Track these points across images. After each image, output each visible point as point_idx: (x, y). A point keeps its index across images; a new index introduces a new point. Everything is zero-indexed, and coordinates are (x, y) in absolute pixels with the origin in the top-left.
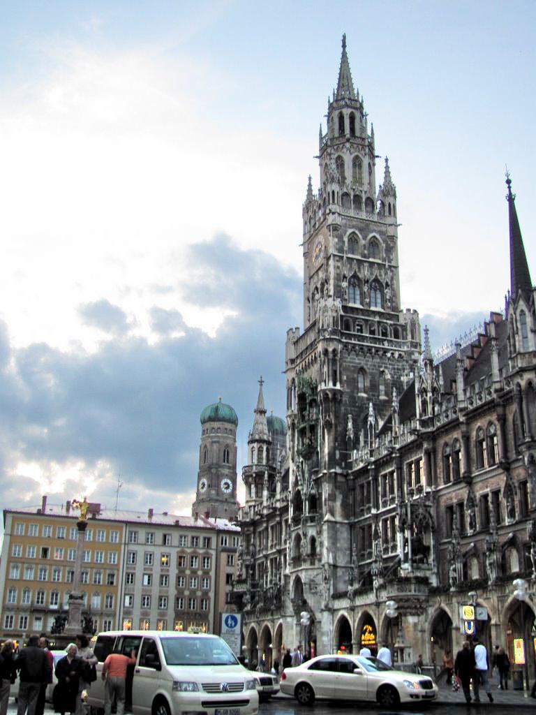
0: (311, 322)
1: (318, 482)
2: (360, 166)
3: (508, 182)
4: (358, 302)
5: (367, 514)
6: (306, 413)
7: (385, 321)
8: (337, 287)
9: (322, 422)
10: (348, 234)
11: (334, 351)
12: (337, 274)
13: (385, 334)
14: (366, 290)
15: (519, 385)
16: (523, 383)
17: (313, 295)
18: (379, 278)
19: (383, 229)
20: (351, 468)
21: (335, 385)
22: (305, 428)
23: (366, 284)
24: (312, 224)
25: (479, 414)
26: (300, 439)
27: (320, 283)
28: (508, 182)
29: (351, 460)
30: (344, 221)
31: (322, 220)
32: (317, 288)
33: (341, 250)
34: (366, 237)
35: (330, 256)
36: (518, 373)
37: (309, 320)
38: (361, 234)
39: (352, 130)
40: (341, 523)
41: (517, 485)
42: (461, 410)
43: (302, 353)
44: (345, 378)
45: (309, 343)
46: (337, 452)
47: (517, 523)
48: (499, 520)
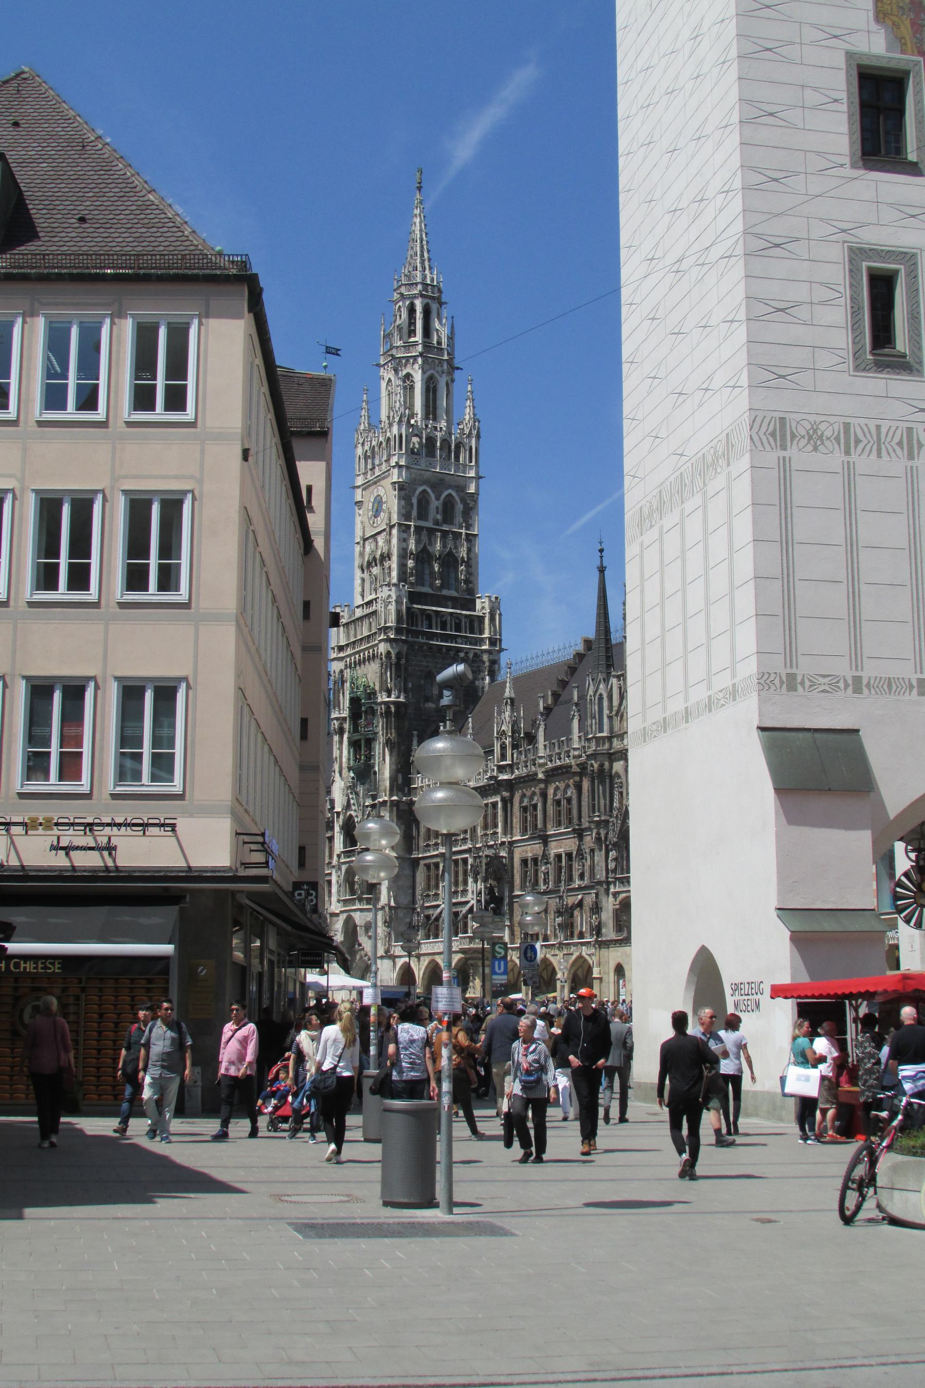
2: (435, 390)
3: (601, 551)
4: (427, 583)
6: (362, 721)
7: (459, 611)
8: (402, 566)
9: (381, 739)
10: (417, 492)
13: (458, 629)
15: (592, 765)
16: (596, 766)
17: (368, 562)
22: (360, 740)
24: (369, 466)
25: (558, 775)
26: (352, 750)
27: (379, 553)
28: (601, 551)
30: (413, 476)
31: (384, 467)
32: (375, 559)
33: (407, 516)
34: (440, 495)
36: (592, 755)
37: (363, 596)
38: (433, 492)
39: (427, 331)
41: (588, 850)
42: (541, 765)
43: (354, 642)
44: (410, 685)
45: (366, 633)
46: (400, 776)
47: (586, 888)
48: (570, 879)
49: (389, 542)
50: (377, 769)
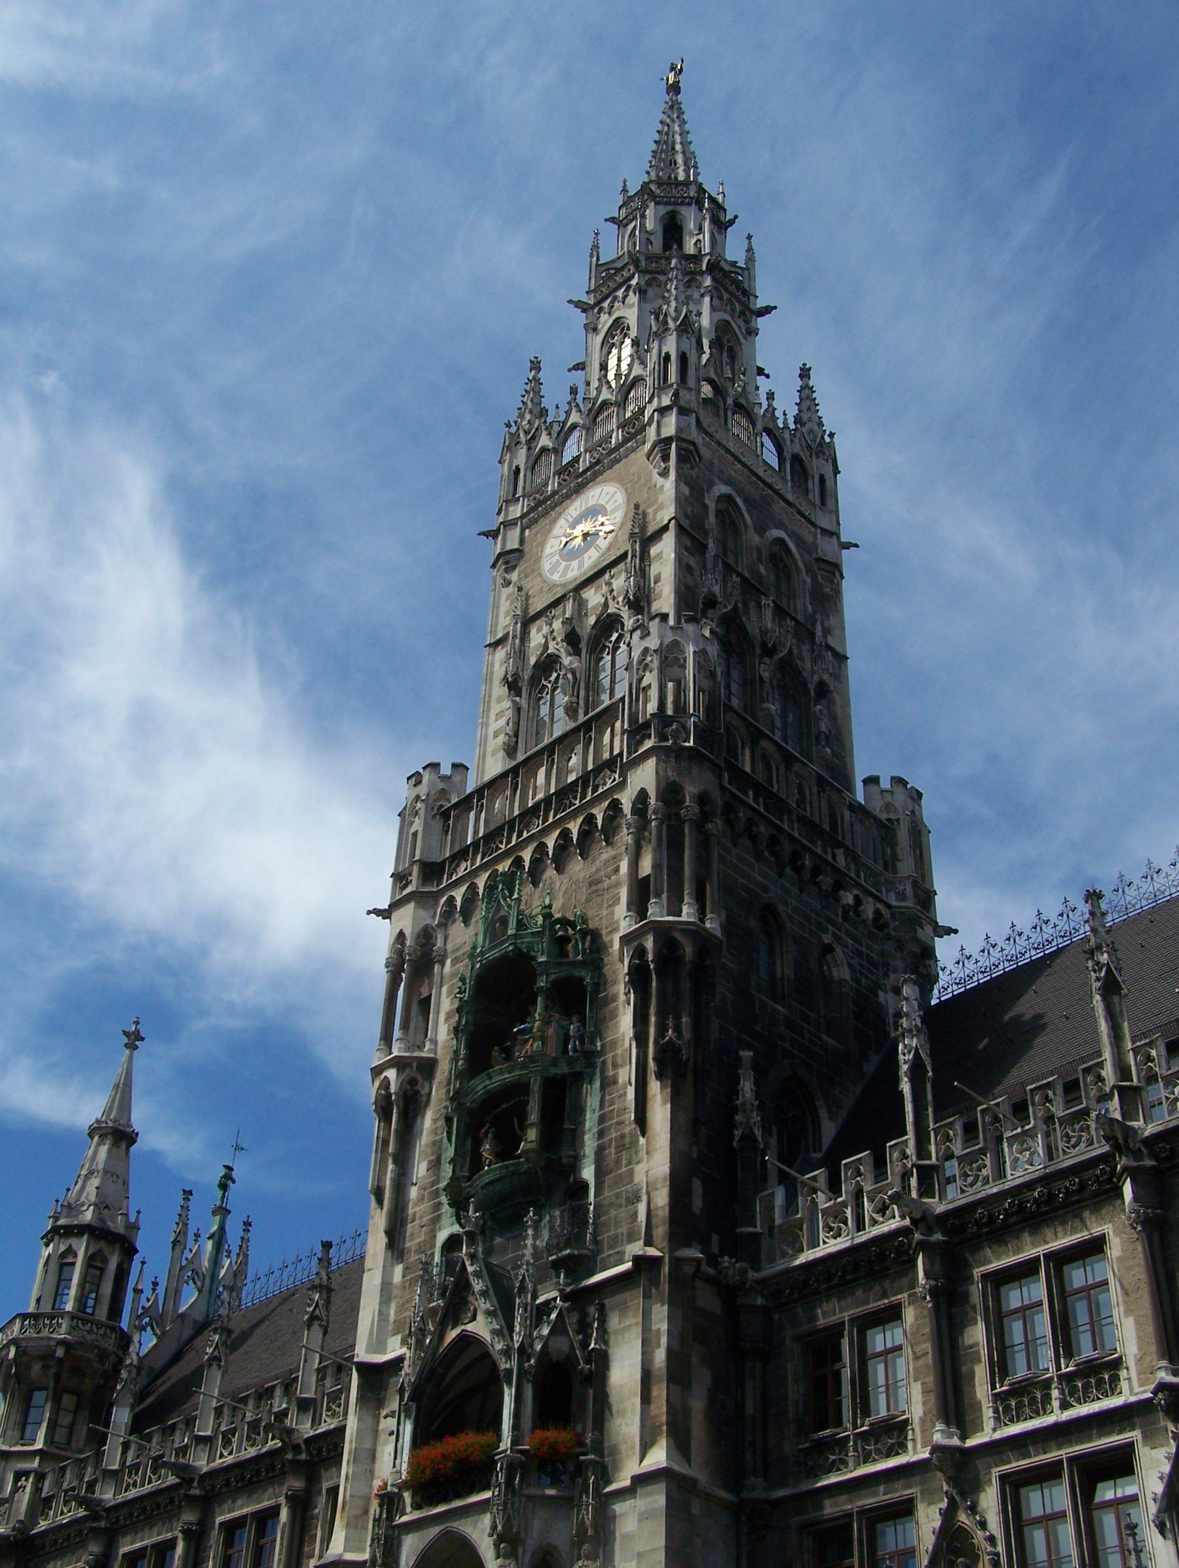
0: (521, 757)
1: (588, 1305)
5: (867, 1459)
11: (703, 799)
12: (687, 587)
14: (766, 675)
18: (799, 663)
19: (806, 533)
20: (756, 1263)
21: (702, 920)
23: (767, 660)
29: (759, 1229)
35: (665, 528)
38: (749, 512)
40: (707, 1497)
46: (697, 1186)
49: (642, 573)
50: (588, 1173)
